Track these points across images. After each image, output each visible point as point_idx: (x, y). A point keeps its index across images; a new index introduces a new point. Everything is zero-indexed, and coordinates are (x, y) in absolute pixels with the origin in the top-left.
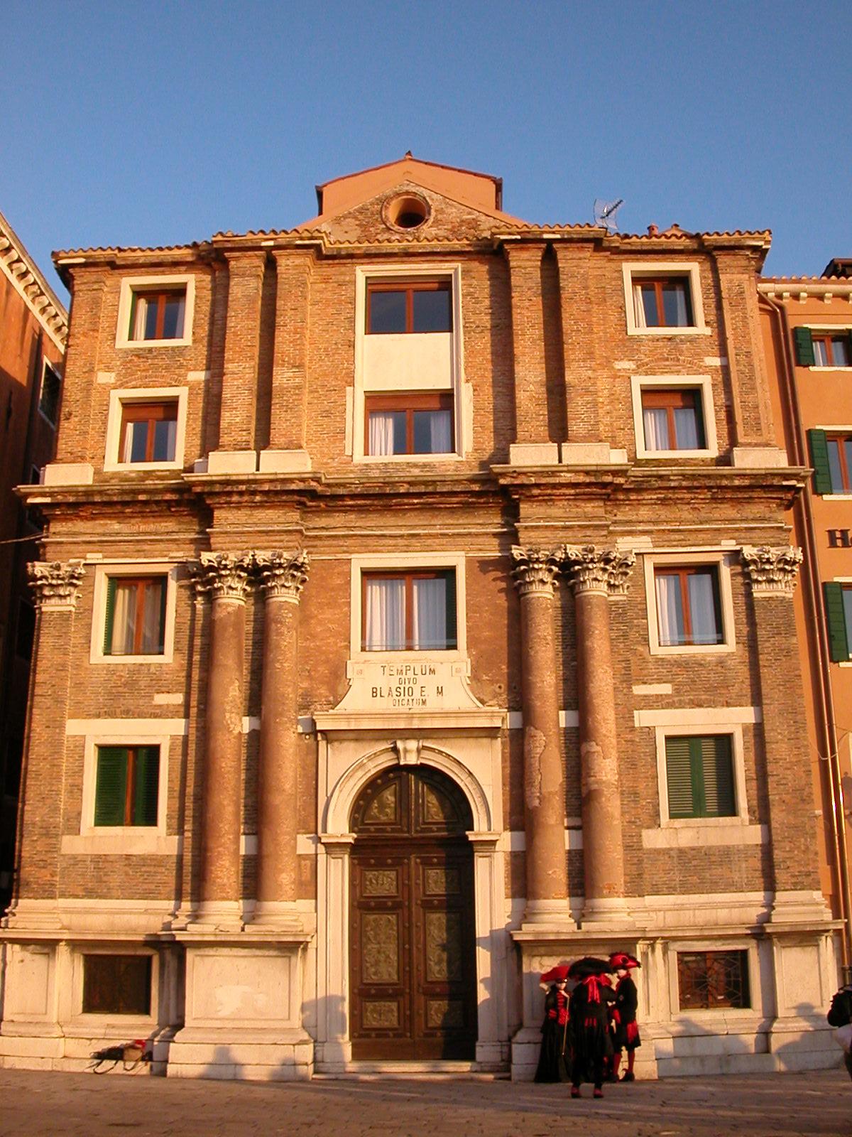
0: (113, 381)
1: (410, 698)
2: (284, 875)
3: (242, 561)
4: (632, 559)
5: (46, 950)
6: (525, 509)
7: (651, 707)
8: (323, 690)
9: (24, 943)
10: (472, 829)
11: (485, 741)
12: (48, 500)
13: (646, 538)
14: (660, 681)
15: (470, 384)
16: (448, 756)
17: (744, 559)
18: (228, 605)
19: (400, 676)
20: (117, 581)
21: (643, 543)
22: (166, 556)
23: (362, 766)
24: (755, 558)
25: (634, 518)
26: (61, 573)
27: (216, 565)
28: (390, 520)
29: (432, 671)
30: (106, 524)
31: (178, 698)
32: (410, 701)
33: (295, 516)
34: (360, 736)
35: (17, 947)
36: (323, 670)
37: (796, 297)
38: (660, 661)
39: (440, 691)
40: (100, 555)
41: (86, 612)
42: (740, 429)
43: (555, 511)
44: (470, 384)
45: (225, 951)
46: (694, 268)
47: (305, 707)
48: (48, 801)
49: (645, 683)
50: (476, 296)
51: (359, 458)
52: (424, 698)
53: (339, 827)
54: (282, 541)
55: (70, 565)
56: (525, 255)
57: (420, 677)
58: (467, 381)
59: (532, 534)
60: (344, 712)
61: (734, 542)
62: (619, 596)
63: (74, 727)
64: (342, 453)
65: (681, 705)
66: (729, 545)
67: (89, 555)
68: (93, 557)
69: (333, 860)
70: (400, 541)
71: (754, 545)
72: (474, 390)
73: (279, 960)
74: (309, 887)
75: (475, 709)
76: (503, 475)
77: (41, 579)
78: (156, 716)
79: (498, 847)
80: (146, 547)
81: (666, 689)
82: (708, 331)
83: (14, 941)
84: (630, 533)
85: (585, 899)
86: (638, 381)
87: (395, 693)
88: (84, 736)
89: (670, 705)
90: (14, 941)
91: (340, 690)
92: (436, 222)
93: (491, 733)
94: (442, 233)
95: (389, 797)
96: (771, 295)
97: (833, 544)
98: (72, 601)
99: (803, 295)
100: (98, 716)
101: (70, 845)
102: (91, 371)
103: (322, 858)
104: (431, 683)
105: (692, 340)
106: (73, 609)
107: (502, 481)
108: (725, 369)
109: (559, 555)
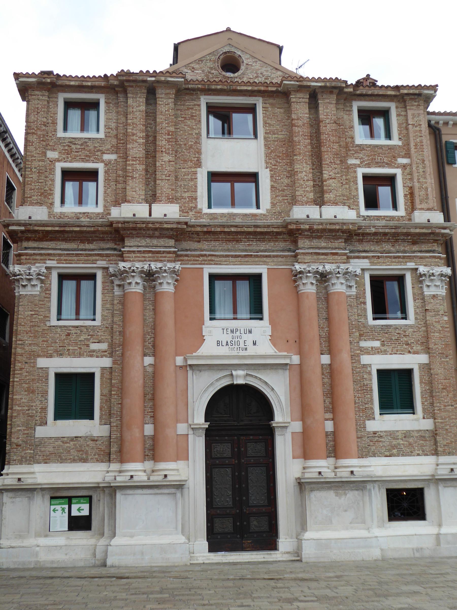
0: (57, 157)
1: (238, 347)
3: (143, 268)
4: (359, 271)
6: (301, 243)
7: (368, 353)
12: (23, 228)
13: (366, 261)
14: (373, 339)
15: (268, 169)
16: (260, 379)
17: (420, 273)
19: (233, 335)
20: (62, 277)
21: (365, 263)
23: (212, 384)
24: (426, 272)
27: (127, 270)
29: (250, 332)
31: (104, 346)
32: (238, 348)
33: (172, 242)
34: (210, 367)
37: (446, 123)
39: (255, 344)
40: (55, 262)
42: (417, 201)
44: (268, 169)
45: (139, 491)
46: (393, 106)
52: (246, 347)
55: (37, 267)
56: (299, 95)
57: (243, 335)
58: (267, 168)
60: (199, 354)
61: (414, 264)
63: (42, 362)
64: (196, 207)
65: (385, 352)
66: (411, 265)
67: (48, 262)
68: (50, 263)
69: (197, 438)
71: (425, 265)
75: (274, 354)
76: (290, 223)
77: (19, 275)
81: (377, 344)
82: (400, 143)
84: (358, 257)
85: (336, 459)
86: (361, 172)
87: (229, 344)
96: (433, 122)
99: (451, 123)
103: (191, 437)
104: (250, 338)
105: (391, 148)
107: (290, 227)
108: (411, 165)
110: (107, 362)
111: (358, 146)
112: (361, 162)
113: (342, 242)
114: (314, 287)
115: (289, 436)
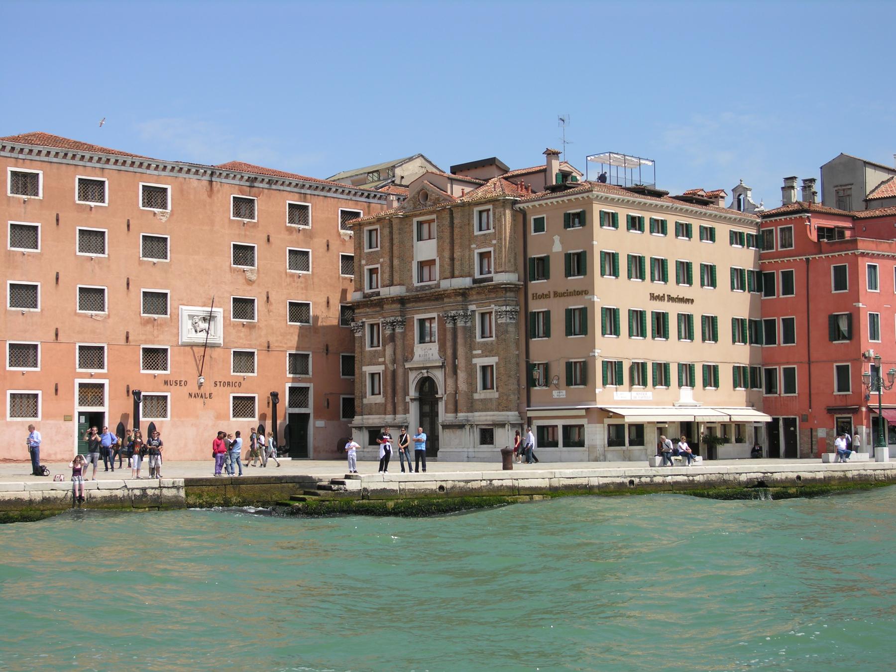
7: (476, 357)
12: (351, 305)
13: (474, 306)
14: (479, 349)
23: (416, 377)
28: (421, 304)
36: (410, 350)
38: (478, 343)
41: (364, 335)
42: (497, 267)
43: (452, 300)
47: (406, 360)
51: (416, 284)
53: (413, 393)
62: (469, 324)
63: (365, 368)
70: (423, 311)
74: (406, 411)
81: (479, 352)
83: (354, 427)
86: (477, 251)
89: (480, 357)
90: (354, 427)
92: (430, 199)
93: (441, 367)
95: (427, 384)
97: (533, 299)
100: (368, 365)
101: (365, 401)
102: (360, 261)
109: (449, 315)
110: (382, 367)
114: (451, 323)
115: (443, 401)
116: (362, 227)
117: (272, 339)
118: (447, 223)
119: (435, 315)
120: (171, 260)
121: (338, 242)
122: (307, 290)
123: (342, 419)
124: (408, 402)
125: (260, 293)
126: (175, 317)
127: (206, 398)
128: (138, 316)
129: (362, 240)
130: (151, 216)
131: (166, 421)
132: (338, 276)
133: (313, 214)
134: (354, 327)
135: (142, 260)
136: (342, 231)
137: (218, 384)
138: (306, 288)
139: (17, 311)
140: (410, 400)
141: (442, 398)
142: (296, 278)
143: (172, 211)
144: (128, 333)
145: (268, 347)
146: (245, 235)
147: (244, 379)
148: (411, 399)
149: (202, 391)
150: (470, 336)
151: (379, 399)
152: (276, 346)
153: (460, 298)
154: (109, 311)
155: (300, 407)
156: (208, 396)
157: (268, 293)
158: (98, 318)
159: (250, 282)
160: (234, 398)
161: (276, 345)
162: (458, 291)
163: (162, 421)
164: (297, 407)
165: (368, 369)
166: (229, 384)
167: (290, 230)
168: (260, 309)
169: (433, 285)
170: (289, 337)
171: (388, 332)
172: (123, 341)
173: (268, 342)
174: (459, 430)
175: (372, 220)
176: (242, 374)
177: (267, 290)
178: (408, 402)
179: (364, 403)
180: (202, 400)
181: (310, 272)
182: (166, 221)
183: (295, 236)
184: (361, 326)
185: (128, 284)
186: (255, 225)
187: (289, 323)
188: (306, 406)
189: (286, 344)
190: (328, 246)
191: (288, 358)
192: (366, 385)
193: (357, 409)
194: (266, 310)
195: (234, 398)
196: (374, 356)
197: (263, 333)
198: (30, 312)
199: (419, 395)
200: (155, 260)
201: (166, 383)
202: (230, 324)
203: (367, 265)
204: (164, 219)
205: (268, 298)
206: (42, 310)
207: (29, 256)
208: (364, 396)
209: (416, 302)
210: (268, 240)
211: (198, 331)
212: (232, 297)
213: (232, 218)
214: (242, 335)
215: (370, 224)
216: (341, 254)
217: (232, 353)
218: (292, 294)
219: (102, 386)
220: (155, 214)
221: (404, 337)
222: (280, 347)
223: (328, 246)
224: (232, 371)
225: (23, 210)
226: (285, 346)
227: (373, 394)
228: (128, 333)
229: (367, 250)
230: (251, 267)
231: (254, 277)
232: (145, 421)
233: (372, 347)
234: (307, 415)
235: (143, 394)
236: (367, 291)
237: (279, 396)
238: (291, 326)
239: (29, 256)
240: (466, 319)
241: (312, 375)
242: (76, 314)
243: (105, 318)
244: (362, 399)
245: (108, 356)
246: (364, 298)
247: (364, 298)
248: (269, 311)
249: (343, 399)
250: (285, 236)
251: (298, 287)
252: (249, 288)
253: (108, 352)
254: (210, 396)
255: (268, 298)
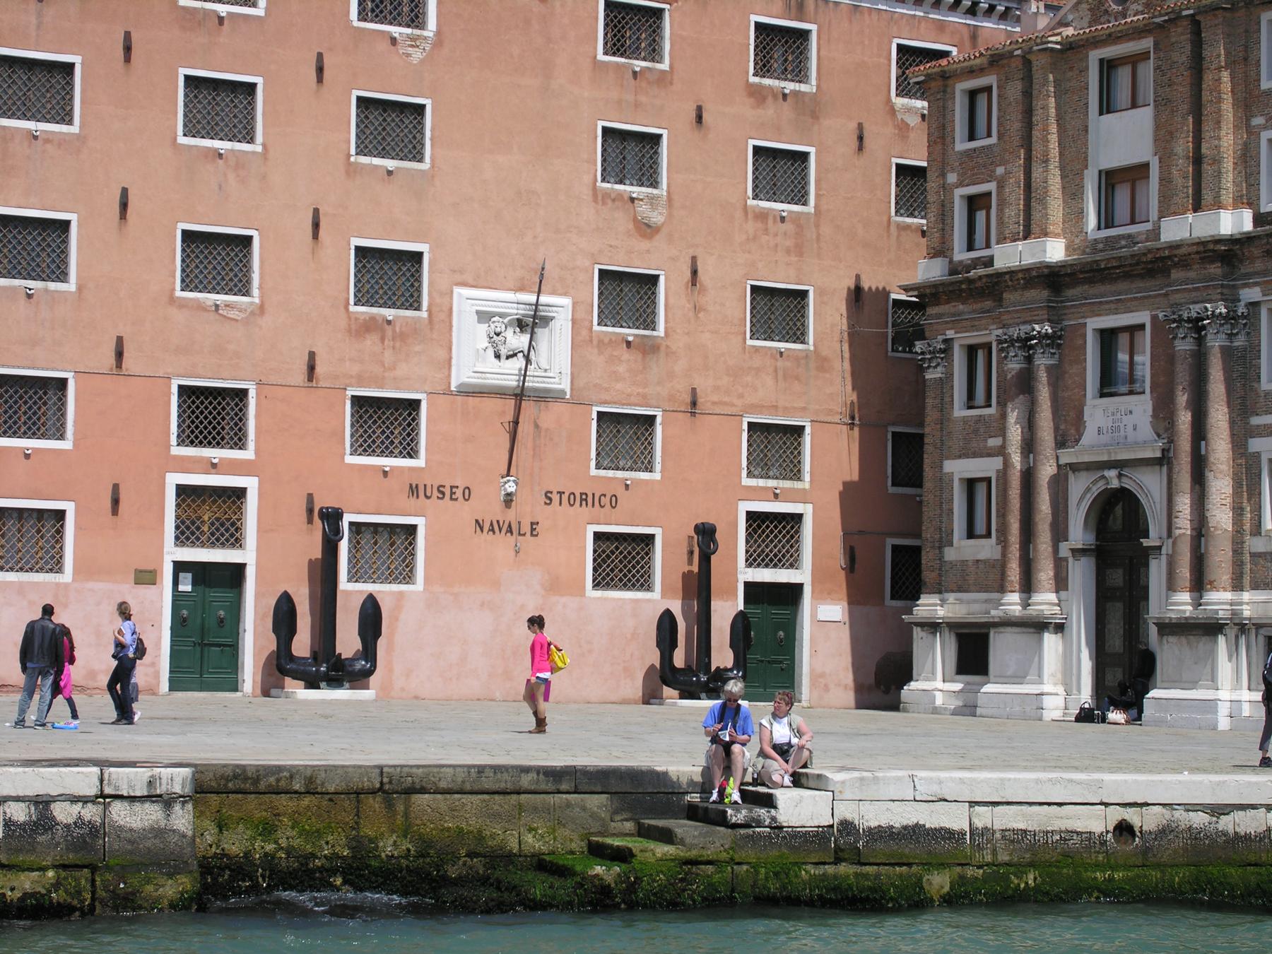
2: (1042, 574)
5: (932, 630)
7: (1260, 435)
8: (1073, 431)
9: (922, 625)
10: (1147, 536)
11: (1157, 468)
13: (1257, 289)
18: (1013, 369)
22: (987, 329)
23: (1088, 490)
25: (1252, 270)
26: (931, 349)
28: (1107, 288)
30: (955, 306)
35: (919, 629)
36: (1072, 414)
41: (949, 375)
43: (1192, 274)
45: (1009, 629)
48: (934, 523)
49: (1257, 415)
50: (1163, 68)
54: (1038, 315)
57: (1124, 417)
59: (1177, 296)
62: (1240, 342)
67: (948, 332)
70: (1113, 306)
72: (1160, 162)
73: (1036, 635)
78: (989, 455)
79: (1164, 551)
80: (976, 323)
88: (953, 473)
90: (917, 624)
91: (1082, 429)
94: (1140, 8)
95: (1119, 510)
98: (939, 369)
100: (960, 457)
101: (950, 554)
103: (1071, 560)
106: (944, 375)
109: (1185, 316)
110: (997, 463)
111: (1264, 92)
112: (1267, 122)
113: (1218, 267)
114: (1189, 340)
115: (1164, 558)
116: (950, 82)
117: (704, 384)
118: (1184, 58)
119: (1143, 317)
120: (433, 165)
121: (890, 130)
122: (800, 254)
123: (889, 602)
124: (1066, 559)
125: (673, 259)
126: (443, 316)
127: (520, 534)
128: (342, 309)
129: (948, 117)
130: (384, 45)
131: (412, 592)
132: (885, 219)
133: (822, 53)
134: (923, 353)
135: (356, 163)
136: (900, 102)
137: (556, 498)
138: (799, 250)
139: (13, 289)
140: (1069, 554)
141: (1159, 548)
142: (770, 221)
143: (439, 33)
144: (312, 355)
145: (694, 404)
146: (637, 105)
147: (627, 486)
148: (1073, 550)
149: (511, 515)
150: (1244, 376)
151: (986, 549)
152: (714, 403)
153: (1215, 269)
154: (262, 297)
155: (775, 566)
156: (526, 528)
157: (694, 259)
158: (232, 314)
159: (646, 230)
160: (598, 536)
161: (715, 398)
162: (1211, 246)
163: (401, 593)
164: (767, 566)
165: (960, 468)
166: (584, 498)
167: (758, 95)
168: (671, 301)
169: (1139, 233)
170: (749, 379)
171: (1014, 366)
172: (299, 376)
173: (694, 390)
174: (1204, 639)
175: (978, 61)
176: (620, 474)
177: (691, 252)
178: (1066, 559)
179: (947, 558)
180: (511, 539)
181: (810, 208)
182: (422, 62)
183: (770, 111)
184: (941, 351)
185: (316, 226)
186: (663, 79)
187: (750, 342)
188: (794, 564)
189: (741, 396)
190: (861, 138)
191: (745, 436)
192: (951, 511)
193: (928, 576)
194: (690, 306)
195: (598, 536)
196: (976, 431)
197: (680, 366)
198: (46, 290)
199: (1097, 539)
200: (390, 164)
201: (414, 490)
202: (591, 341)
203: (961, 184)
204: (417, 55)
205: (694, 273)
206: (80, 288)
207: (47, 141)
208: (945, 540)
209: (1091, 281)
210: (699, 118)
211: (503, 357)
212: (597, 267)
213: (601, 57)
214: (621, 369)
215: (972, 72)
216: (895, 160)
217: (595, 416)
218: (760, 265)
219: (240, 493)
220: (394, 41)
221: (1057, 378)
222: (725, 404)
223: (861, 138)
224: (593, 464)
225: (34, 20)
226: (739, 402)
227: (971, 534)
228: (312, 355)
229: (961, 145)
230: (650, 190)
231: (657, 218)
232: (350, 590)
233: (970, 407)
234: (795, 590)
235: (347, 518)
236: (961, 255)
237: (717, 535)
238: (757, 349)
239: (47, 141)
240: (1233, 327)
241: (812, 481)
242: (172, 300)
243: (252, 313)
244: (940, 548)
245: (257, 416)
246: (950, 275)
247: (950, 275)
248: (697, 309)
249: (895, 548)
250: (744, 108)
251: (776, 245)
252: (644, 245)
253: (258, 405)
254: (533, 530)
255: (694, 273)
